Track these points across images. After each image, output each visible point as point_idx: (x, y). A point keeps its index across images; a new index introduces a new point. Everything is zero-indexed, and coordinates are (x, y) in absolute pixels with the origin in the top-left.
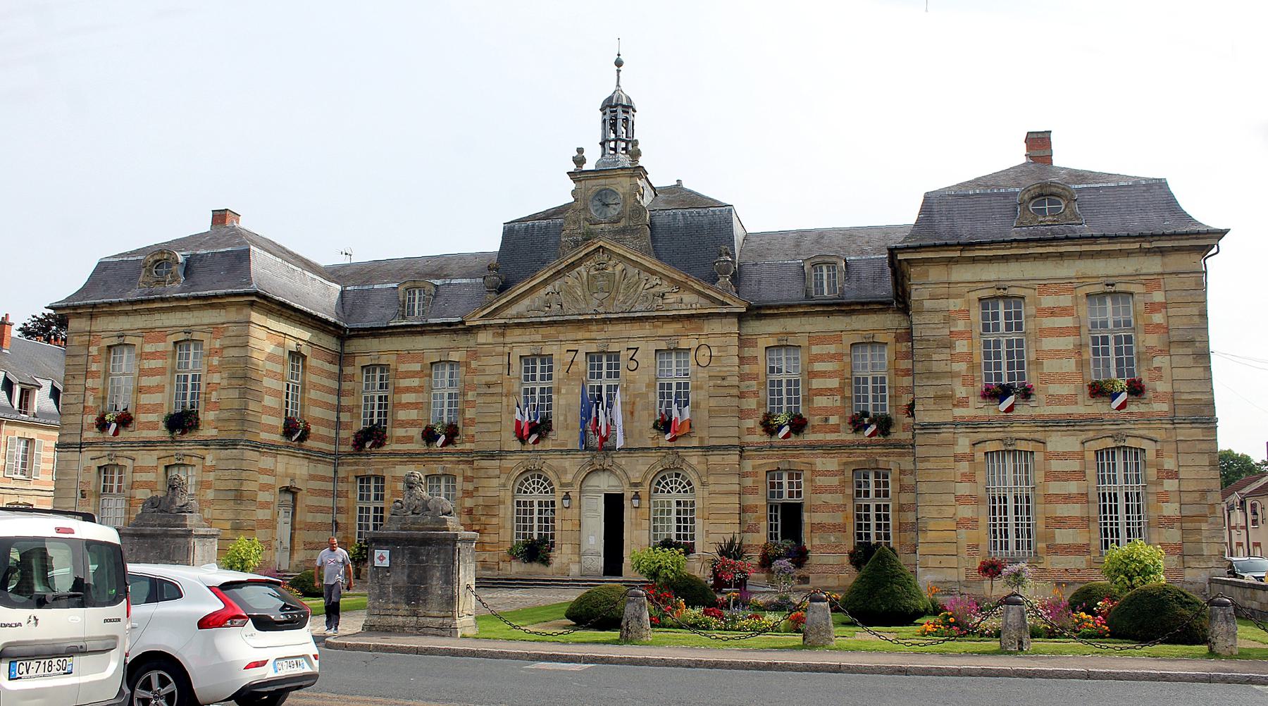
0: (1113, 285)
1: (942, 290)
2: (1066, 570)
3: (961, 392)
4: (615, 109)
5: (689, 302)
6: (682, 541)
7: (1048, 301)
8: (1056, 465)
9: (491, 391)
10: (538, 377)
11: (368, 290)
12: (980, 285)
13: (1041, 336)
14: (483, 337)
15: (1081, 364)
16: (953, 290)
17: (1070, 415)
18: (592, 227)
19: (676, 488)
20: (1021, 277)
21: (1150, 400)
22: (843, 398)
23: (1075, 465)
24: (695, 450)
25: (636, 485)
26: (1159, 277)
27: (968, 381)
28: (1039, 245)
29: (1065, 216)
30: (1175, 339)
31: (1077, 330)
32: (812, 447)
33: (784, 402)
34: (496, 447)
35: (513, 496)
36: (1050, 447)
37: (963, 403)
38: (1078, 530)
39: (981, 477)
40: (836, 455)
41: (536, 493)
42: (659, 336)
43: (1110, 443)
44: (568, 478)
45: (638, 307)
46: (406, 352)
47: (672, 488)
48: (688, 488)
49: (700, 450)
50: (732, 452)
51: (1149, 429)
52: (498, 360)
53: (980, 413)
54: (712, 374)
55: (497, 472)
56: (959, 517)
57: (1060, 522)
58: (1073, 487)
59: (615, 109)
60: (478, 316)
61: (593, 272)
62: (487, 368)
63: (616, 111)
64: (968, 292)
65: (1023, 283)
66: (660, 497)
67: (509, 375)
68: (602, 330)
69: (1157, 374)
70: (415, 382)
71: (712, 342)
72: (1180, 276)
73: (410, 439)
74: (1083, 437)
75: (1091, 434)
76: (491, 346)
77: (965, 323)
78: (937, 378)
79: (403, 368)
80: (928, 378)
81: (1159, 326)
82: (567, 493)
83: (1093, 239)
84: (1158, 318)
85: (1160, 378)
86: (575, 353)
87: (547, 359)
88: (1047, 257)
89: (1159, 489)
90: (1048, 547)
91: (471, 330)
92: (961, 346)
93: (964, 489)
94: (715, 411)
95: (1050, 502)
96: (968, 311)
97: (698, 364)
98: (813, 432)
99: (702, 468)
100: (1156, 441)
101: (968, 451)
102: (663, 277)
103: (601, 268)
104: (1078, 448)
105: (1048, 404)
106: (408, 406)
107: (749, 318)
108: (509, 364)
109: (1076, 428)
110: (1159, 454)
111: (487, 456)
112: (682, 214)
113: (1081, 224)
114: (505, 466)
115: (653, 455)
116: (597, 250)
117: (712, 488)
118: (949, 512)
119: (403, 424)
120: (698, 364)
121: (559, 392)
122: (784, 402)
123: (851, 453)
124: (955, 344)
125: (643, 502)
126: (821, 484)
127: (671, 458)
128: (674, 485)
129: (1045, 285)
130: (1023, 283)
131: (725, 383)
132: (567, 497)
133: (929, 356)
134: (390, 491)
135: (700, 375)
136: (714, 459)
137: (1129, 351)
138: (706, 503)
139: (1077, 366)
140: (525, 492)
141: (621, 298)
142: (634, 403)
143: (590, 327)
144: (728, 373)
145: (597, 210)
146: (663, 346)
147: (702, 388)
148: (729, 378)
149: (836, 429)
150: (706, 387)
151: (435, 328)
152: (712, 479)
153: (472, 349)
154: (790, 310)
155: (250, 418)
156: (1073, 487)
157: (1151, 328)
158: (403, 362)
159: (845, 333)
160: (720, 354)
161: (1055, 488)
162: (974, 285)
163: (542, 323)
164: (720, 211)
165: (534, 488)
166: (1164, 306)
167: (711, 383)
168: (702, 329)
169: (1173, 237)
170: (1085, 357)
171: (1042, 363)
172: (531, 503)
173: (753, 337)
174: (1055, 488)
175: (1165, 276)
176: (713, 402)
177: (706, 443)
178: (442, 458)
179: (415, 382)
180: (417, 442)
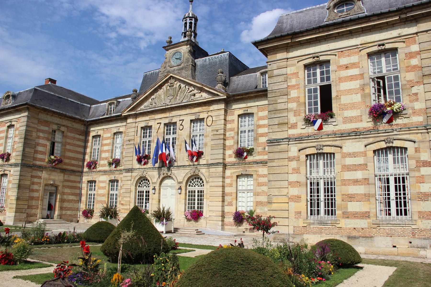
0: (383, 45)
1: (283, 63)
2: (355, 228)
3: (293, 119)
5: (205, 97)
6: (199, 210)
7: (344, 61)
8: (349, 161)
10: (148, 136)
11: (99, 106)
12: (304, 58)
13: (340, 82)
14: (129, 121)
15: (365, 96)
16: (290, 62)
17: (358, 129)
20: (328, 49)
21: (410, 115)
23: (360, 160)
24: (205, 166)
25: (180, 183)
26: (415, 35)
27: (296, 113)
28: (335, 27)
29: (354, 10)
30: (426, 74)
31: (361, 76)
32: (257, 163)
34: (130, 167)
35: (136, 189)
36: (345, 150)
37: (294, 126)
38: (363, 203)
39: (303, 170)
41: (145, 187)
42: (192, 114)
43: (383, 145)
44: (155, 180)
45: (184, 101)
47: (196, 184)
48: (202, 184)
49: (206, 166)
50: (220, 166)
51: (409, 134)
52: (133, 130)
53: (303, 131)
54: (213, 129)
55: (130, 178)
56: (290, 195)
57: (351, 197)
58: (359, 175)
61: (168, 88)
64: (298, 62)
65: (329, 53)
66: (190, 188)
69: (414, 97)
72: (429, 32)
74: (367, 141)
75: (371, 140)
77: (296, 80)
78: (280, 113)
79: (106, 135)
80: (275, 113)
81: (415, 67)
82: (155, 187)
83: (367, 18)
84: (415, 62)
85: (417, 100)
86: (160, 124)
87: (150, 127)
88: (343, 35)
89: (417, 174)
90: (343, 213)
91: (126, 118)
92: (294, 93)
93: (293, 178)
94: (214, 147)
95: (345, 185)
96: (298, 73)
97: (207, 125)
98: (258, 155)
99: (206, 174)
100: (415, 142)
101: (296, 154)
102: (194, 86)
104: (362, 149)
105: (344, 122)
107: (231, 102)
108: (137, 131)
109: (361, 136)
110: (417, 150)
113: (364, 13)
115: (188, 168)
117: (210, 184)
118: (284, 192)
120: (207, 125)
124: (290, 92)
126: (261, 181)
127: (194, 170)
128: (197, 183)
129: (342, 51)
130: (329, 53)
131: (218, 133)
132: (154, 189)
133: (276, 100)
135: (208, 130)
136: (212, 170)
137: (397, 85)
138: (208, 191)
139: (362, 98)
141: (178, 98)
142: (181, 145)
145: (174, 61)
146: (193, 118)
147: (208, 136)
150: (210, 135)
151: (114, 118)
152: (211, 180)
154: (247, 96)
155: (27, 155)
156: (359, 175)
157: (410, 69)
158: (105, 133)
160: (216, 119)
161: (348, 175)
162: (300, 58)
163: (148, 112)
164: (224, 55)
165: (144, 185)
166: (418, 53)
167: (212, 134)
168: (209, 108)
169: (421, 7)
170: (367, 91)
171: (340, 99)
173: (233, 110)
174: (348, 175)
175: (418, 34)
176: (213, 142)
177: (210, 162)
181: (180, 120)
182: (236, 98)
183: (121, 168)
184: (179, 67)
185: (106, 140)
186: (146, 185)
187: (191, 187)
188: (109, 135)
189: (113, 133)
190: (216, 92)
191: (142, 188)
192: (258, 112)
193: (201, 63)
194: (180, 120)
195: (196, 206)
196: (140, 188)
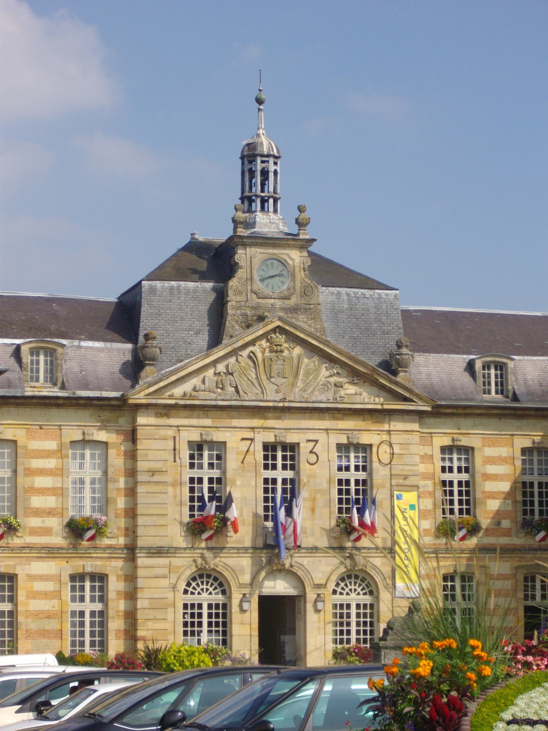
4: (266, 159)
9: (156, 478)
18: (261, 301)
19: (355, 590)
22: (515, 502)
25: (318, 586)
33: (456, 503)
40: (509, 559)
41: (205, 595)
42: (340, 430)
46: (38, 427)
55: (166, 571)
59: (266, 159)
60: (142, 394)
62: (150, 453)
63: (268, 162)
67: (175, 461)
68: (279, 418)
70: (51, 463)
71: (395, 438)
73: (47, 531)
76: (154, 428)
79: (35, 445)
103: (276, 350)
106: (43, 491)
107: (425, 415)
108: (175, 450)
111: (154, 553)
112: (348, 294)
114: (174, 564)
116: (274, 330)
119: (37, 513)
121: (234, 483)
122: (456, 503)
123: (522, 557)
125: (326, 604)
131: (407, 482)
134: (24, 593)
140: (192, 593)
141: (300, 384)
142: (314, 499)
143: (266, 414)
144: (410, 473)
146: (343, 440)
148: (411, 478)
149: (507, 533)
153: (122, 428)
158: (34, 438)
159: (516, 437)
160: (402, 452)
164: (387, 295)
165: (202, 589)
172: (200, 606)
178: (90, 553)
179: (51, 463)
180: (57, 535)
181: (308, 441)
182: (442, 411)
183: (106, 542)
184: (286, 302)
185: (37, 457)
186: (207, 590)
187: (338, 596)
188: (52, 445)
189: (68, 440)
190: (407, 395)
191: (196, 595)
192: (484, 446)
193: (330, 298)
194: (308, 441)
195: (353, 636)
196: (189, 595)
